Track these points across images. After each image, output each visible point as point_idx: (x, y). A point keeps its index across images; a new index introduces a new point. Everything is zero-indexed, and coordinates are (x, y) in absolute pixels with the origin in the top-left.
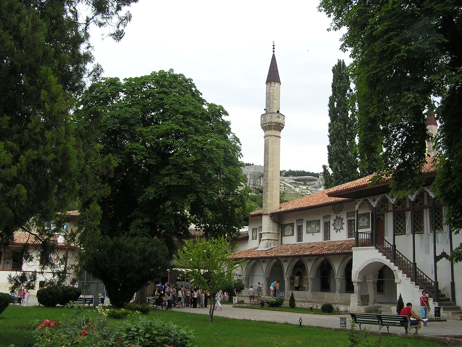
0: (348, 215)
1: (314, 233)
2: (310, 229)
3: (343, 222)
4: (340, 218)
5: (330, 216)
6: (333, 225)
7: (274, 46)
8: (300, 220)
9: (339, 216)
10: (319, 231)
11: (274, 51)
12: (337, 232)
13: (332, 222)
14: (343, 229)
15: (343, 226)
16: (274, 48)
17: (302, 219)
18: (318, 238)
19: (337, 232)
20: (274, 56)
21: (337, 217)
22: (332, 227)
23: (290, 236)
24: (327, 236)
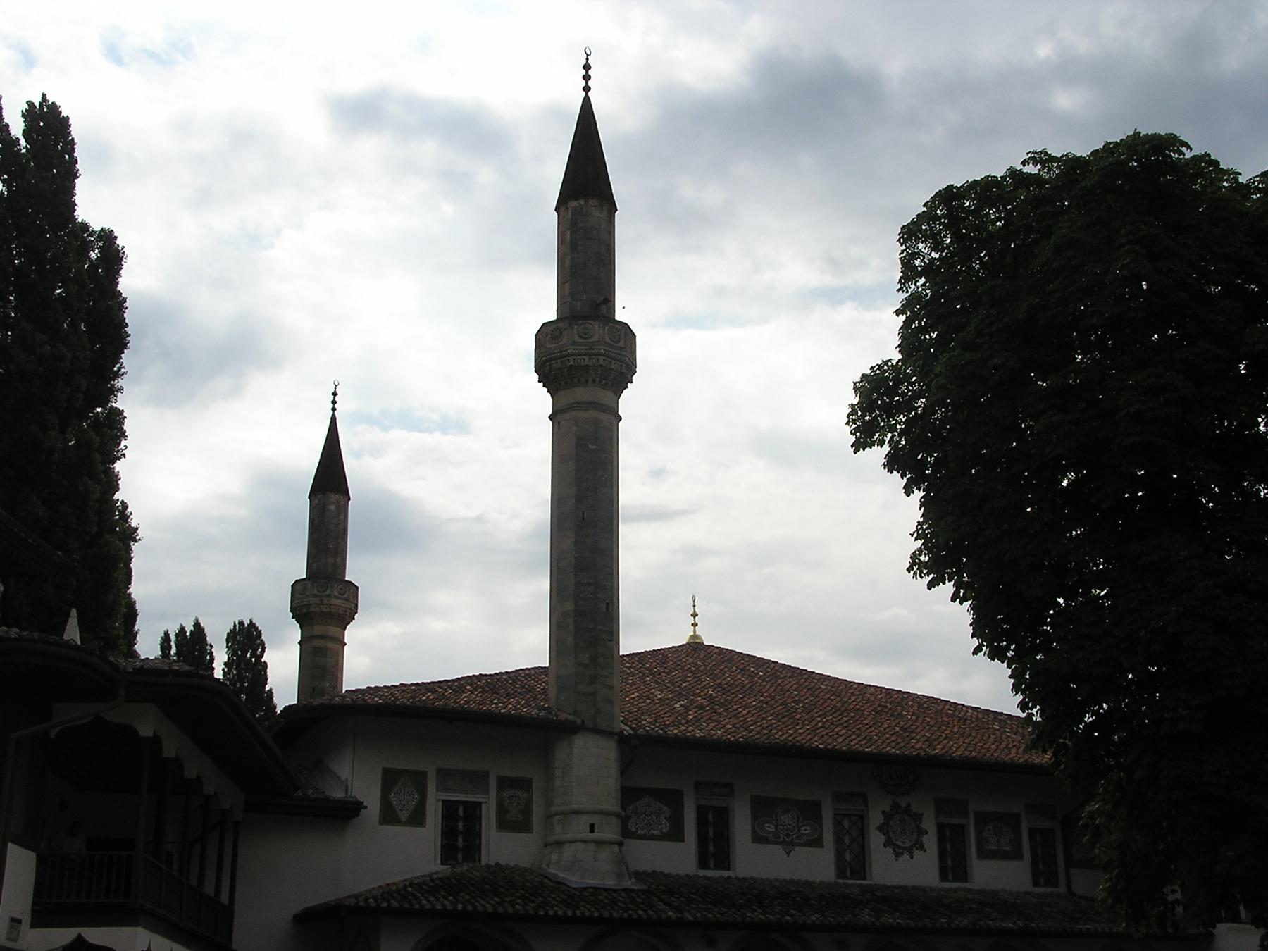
1: (793, 844)
2: (770, 827)
3: (923, 826)
6: (880, 829)
7: (587, 67)
9: (903, 804)
10: (817, 842)
11: (587, 89)
12: (898, 855)
13: (875, 819)
14: (922, 848)
15: (925, 838)
16: (587, 78)
18: (815, 865)
19: (898, 855)
20: (587, 107)
21: (895, 806)
22: (876, 840)
24: (853, 861)
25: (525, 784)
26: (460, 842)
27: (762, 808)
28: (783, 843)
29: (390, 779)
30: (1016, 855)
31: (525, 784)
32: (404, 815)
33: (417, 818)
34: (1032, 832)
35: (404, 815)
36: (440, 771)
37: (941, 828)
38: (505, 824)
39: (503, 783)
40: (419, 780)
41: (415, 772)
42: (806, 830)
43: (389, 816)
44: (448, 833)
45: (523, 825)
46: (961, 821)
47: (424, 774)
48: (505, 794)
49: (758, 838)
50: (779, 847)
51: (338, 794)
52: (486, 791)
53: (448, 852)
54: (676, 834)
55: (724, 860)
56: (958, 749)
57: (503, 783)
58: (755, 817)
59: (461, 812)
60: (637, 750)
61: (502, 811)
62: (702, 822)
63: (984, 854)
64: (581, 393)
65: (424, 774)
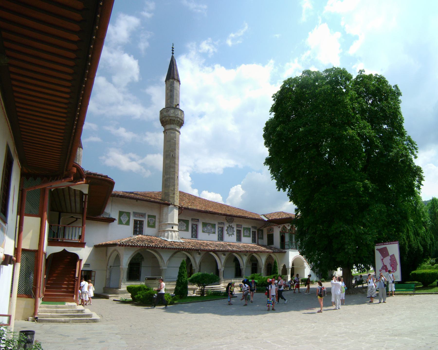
0: (238, 226)
4: (231, 227)
5: (223, 223)
8: (196, 219)
9: (231, 225)
10: (214, 233)
13: (225, 228)
14: (234, 235)
17: (198, 220)
21: (229, 225)
22: (225, 232)
23: (182, 231)
25: (154, 217)
26: (138, 230)
27: (205, 225)
28: (208, 233)
29: (121, 213)
30: (250, 237)
31: (154, 217)
32: (124, 223)
33: (128, 223)
34: (252, 231)
35: (124, 223)
36: (134, 212)
37: (237, 230)
38: (149, 226)
39: (149, 216)
40: (128, 214)
41: (128, 213)
42: (213, 230)
43: (120, 222)
44: (135, 227)
45: (153, 226)
46: (240, 229)
47: (130, 213)
48: (150, 219)
49: (203, 232)
50: (207, 234)
51: (108, 217)
52: (145, 218)
53: (135, 232)
54: (187, 230)
55: (196, 237)
56: (240, 214)
57: (149, 216)
58: (203, 227)
59: (138, 222)
60: (181, 210)
61: (149, 223)
62: (192, 227)
63: (244, 236)
64: (172, 126)
65: (130, 213)
